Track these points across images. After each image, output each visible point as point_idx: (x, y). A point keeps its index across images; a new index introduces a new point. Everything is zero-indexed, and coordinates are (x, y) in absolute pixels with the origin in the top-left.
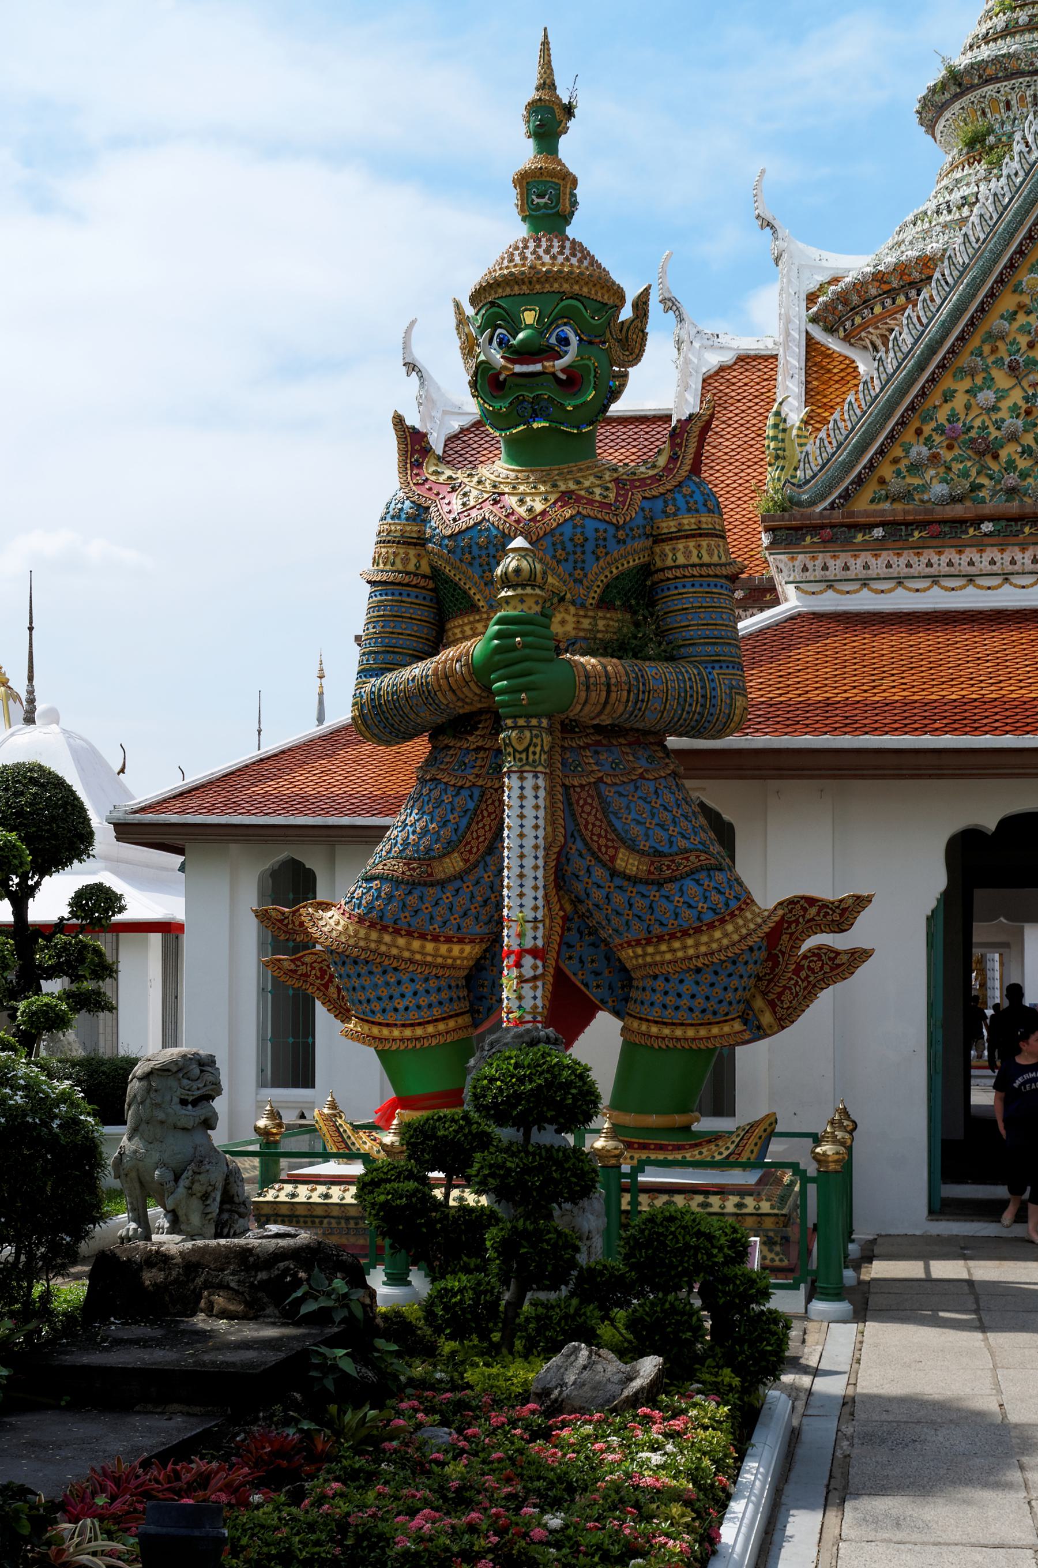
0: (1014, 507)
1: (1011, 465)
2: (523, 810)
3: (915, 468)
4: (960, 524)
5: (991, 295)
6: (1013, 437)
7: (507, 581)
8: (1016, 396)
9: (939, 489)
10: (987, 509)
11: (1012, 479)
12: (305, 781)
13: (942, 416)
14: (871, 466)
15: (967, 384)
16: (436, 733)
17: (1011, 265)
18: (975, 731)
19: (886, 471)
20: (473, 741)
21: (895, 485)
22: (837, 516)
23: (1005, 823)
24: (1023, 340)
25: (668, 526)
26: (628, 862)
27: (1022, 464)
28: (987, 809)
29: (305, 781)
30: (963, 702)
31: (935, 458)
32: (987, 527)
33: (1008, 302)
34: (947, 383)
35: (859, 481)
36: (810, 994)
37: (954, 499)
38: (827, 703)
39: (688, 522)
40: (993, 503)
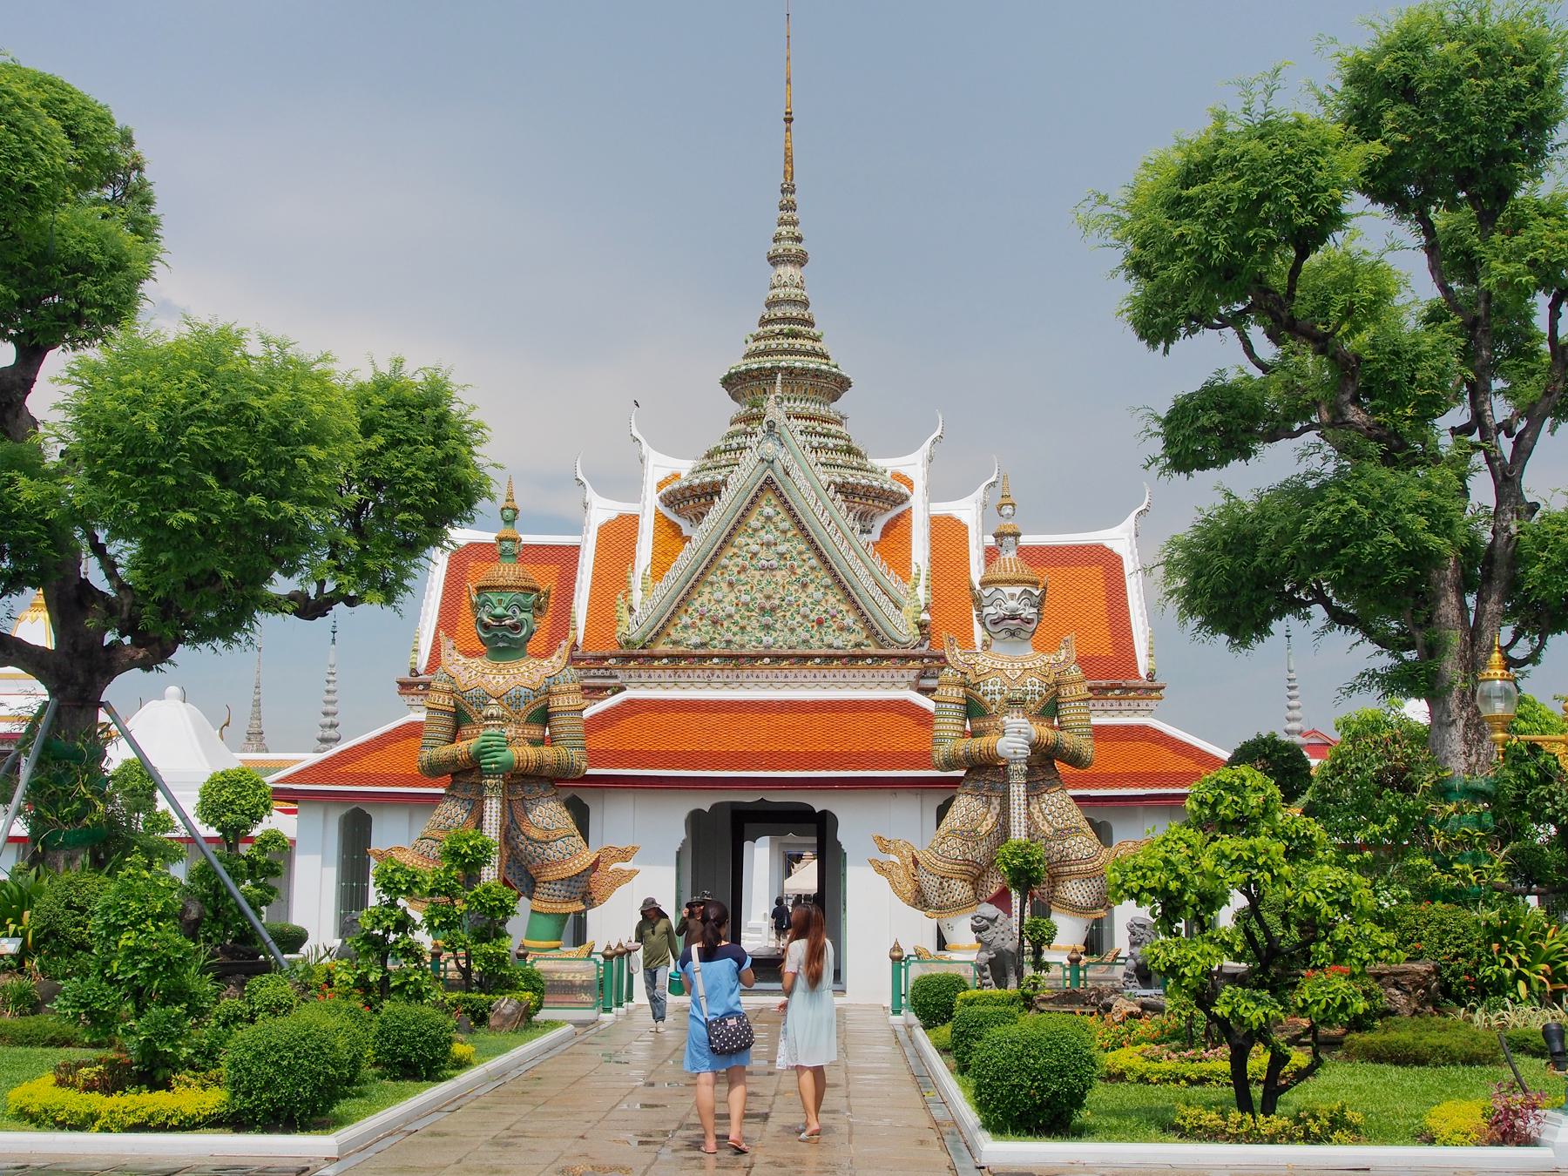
0: (727, 652)
1: (728, 629)
2: (493, 810)
3: (686, 627)
4: (703, 658)
5: (720, 548)
6: (730, 616)
7: (487, 718)
8: (732, 596)
9: (695, 640)
10: (716, 652)
11: (729, 636)
12: (367, 765)
13: (697, 604)
14: (663, 627)
15: (708, 589)
16: (453, 775)
17: (730, 535)
18: (695, 768)
19: (672, 632)
20: (472, 779)
21: (675, 635)
22: (645, 652)
23: (714, 807)
24: (736, 569)
25: (555, 689)
26: (535, 834)
27: (735, 629)
28: (705, 803)
29: (367, 765)
30: (693, 752)
31: (693, 625)
32: (716, 660)
33: (730, 551)
34: (700, 588)
35: (657, 634)
36: (614, 886)
37: (703, 645)
38: (632, 751)
39: (564, 688)
40: (718, 647)
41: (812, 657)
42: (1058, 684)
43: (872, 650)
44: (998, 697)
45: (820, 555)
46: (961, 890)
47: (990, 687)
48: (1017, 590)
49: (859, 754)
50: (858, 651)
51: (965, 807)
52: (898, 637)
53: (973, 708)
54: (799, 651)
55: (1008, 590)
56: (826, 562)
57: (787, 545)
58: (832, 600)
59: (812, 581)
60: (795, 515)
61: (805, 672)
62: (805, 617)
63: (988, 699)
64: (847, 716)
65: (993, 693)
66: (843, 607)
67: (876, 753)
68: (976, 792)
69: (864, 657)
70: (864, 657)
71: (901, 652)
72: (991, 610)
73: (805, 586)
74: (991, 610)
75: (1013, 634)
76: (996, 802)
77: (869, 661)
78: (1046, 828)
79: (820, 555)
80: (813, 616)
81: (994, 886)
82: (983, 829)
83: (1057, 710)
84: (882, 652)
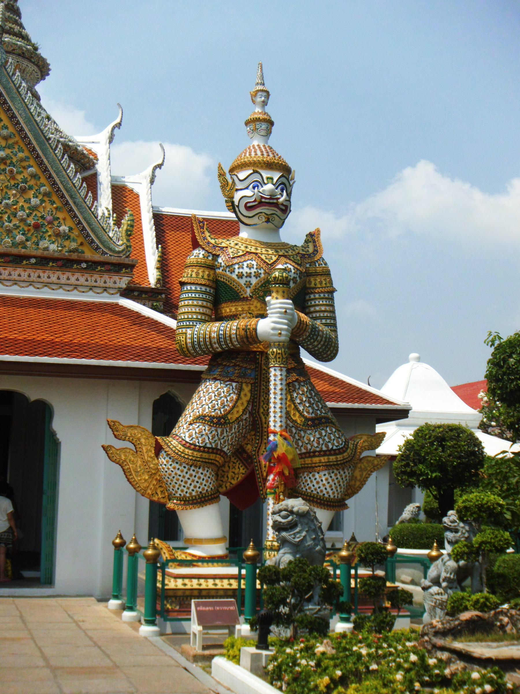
41: (28, 257)
42: (308, 274)
43: (88, 254)
44: (254, 281)
45: (41, 164)
46: (202, 481)
47: (246, 270)
48: (276, 176)
49: (80, 345)
50: (74, 256)
51: (210, 397)
52: (112, 246)
53: (220, 295)
54: (15, 251)
55: (266, 174)
56: (46, 170)
57: (8, 151)
58: (49, 207)
59: (31, 188)
60: (18, 123)
61: (19, 271)
62: (22, 220)
63: (242, 281)
64: (61, 313)
65: (249, 275)
66: (60, 215)
67: (97, 345)
68: (225, 378)
69: (79, 262)
70: (79, 262)
71: (114, 259)
72: (248, 193)
73: (23, 191)
74: (248, 193)
75: (268, 221)
76: (247, 389)
77: (84, 265)
78: (297, 417)
79: (41, 164)
80: (31, 221)
81: (237, 473)
82: (234, 416)
83: (305, 301)
84: (97, 257)
